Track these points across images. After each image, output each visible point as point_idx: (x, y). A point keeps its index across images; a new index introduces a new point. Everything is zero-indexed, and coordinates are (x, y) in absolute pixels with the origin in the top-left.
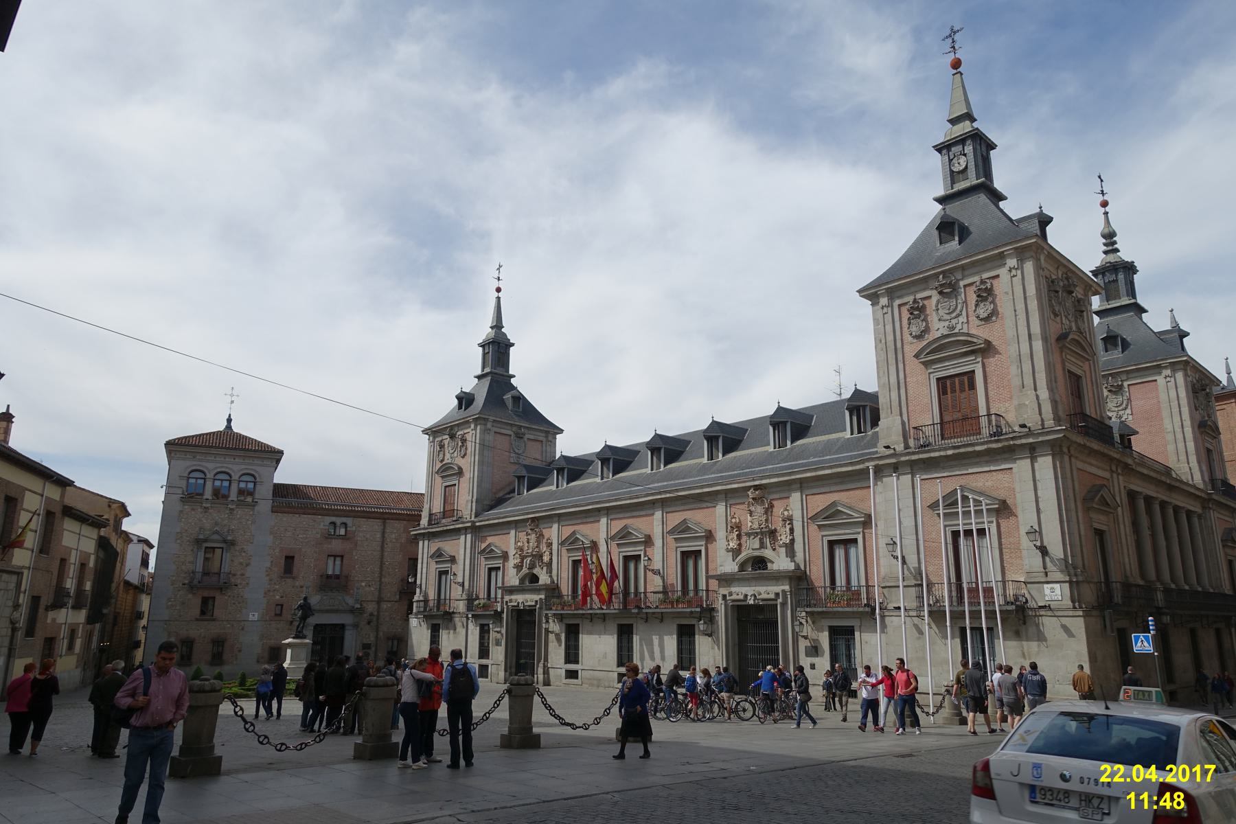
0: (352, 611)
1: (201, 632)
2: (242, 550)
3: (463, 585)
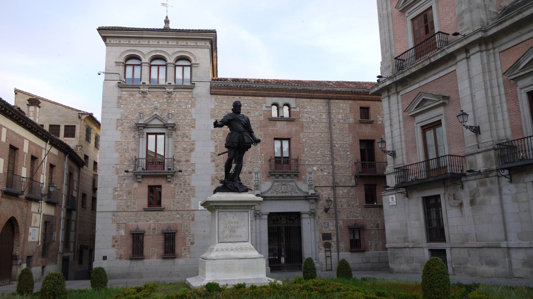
0: (306, 198)
1: (152, 223)
2: (185, 136)
3: (477, 130)
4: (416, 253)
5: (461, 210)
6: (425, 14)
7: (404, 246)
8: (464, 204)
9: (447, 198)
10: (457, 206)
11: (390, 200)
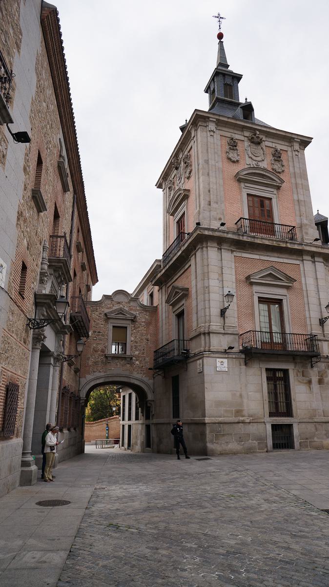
4: (253, 429)
5: (310, 387)
6: (262, 199)
7: (237, 421)
8: (313, 381)
9: (295, 373)
10: (306, 383)
11: (218, 364)
